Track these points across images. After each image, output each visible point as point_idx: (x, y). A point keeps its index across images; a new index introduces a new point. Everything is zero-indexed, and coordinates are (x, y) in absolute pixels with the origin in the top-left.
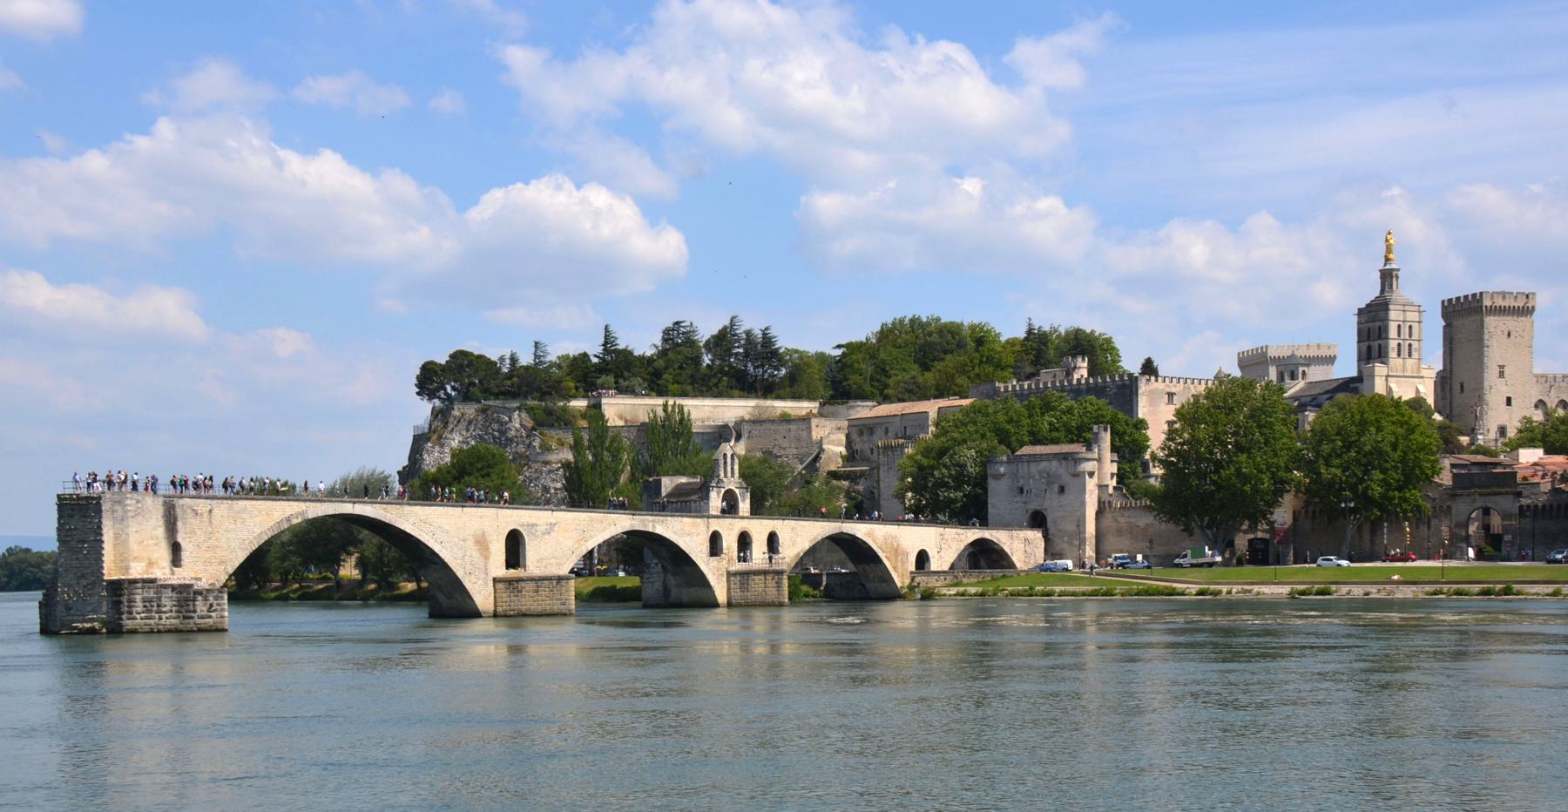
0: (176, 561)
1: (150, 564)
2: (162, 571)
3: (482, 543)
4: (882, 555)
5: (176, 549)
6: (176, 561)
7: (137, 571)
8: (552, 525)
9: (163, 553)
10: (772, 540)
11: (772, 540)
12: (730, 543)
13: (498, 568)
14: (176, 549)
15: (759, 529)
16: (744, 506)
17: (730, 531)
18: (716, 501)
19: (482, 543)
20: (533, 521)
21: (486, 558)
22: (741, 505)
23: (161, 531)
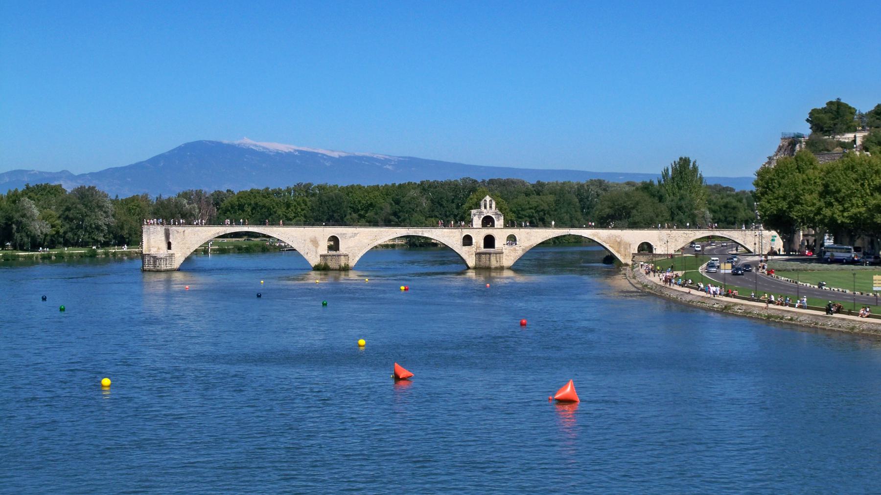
0: (169, 247)
1: (159, 249)
2: (163, 252)
3: (315, 242)
4: (607, 246)
6: (169, 247)
7: (153, 252)
8: (356, 234)
9: (165, 246)
10: (512, 239)
11: (512, 239)
13: (323, 249)
15: (500, 234)
16: (499, 222)
17: (478, 235)
18: (477, 221)
21: (317, 247)
22: (496, 222)
23: (163, 238)
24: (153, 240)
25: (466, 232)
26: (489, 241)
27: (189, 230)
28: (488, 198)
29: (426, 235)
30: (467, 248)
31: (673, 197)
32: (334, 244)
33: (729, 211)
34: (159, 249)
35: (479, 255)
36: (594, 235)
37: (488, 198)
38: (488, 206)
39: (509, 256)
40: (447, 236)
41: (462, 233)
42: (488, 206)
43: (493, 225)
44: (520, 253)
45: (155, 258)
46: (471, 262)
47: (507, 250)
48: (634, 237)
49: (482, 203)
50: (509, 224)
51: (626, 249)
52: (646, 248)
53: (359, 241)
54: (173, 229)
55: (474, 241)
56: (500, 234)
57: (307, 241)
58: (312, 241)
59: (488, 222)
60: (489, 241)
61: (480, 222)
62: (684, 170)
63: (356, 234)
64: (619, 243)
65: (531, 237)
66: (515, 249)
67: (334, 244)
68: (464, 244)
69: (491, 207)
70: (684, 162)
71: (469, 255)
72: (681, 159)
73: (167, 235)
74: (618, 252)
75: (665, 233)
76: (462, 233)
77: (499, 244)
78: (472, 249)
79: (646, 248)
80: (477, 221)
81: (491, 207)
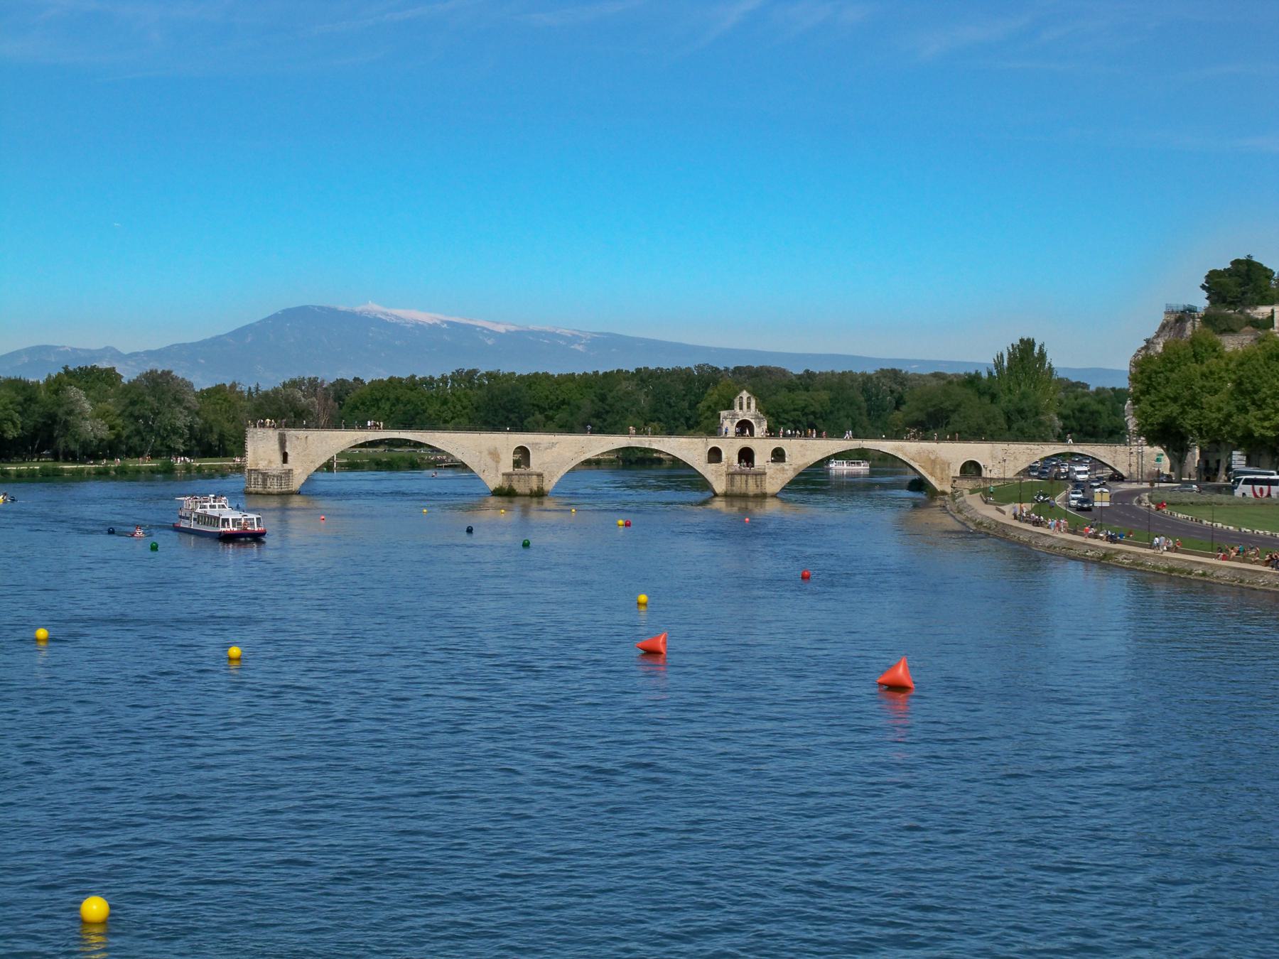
0: (285, 460)
1: (270, 462)
2: (276, 466)
3: (495, 455)
6: (285, 460)
7: (262, 465)
8: (553, 445)
9: (279, 458)
10: (778, 455)
11: (778, 455)
13: (507, 465)
16: (760, 430)
17: (730, 448)
18: (729, 425)
21: (498, 462)
22: (756, 430)
23: (277, 447)
24: (261, 448)
25: (713, 442)
26: (746, 455)
27: (314, 435)
28: (745, 394)
29: (655, 447)
31: (1014, 395)
32: (523, 455)
33: (1090, 417)
34: (270, 462)
35: (731, 475)
36: (897, 449)
37: (745, 394)
38: (745, 406)
39: (776, 478)
40: (687, 449)
41: (707, 445)
42: (745, 406)
43: (752, 434)
44: (790, 475)
45: (265, 476)
46: (720, 486)
47: (771, 469)
48: (956, 453)
49: (737, 401)
50: (772, 432)
51: (943, 470)
52: (971, 469)
53: (559, 453)
54: (291, 433)
55: (724, 456)
56: (762, 447)
57: (484, 452)
59: (744, 427)
60: (746, 455)
62: (1026, 357)
63: (553, 445)
64: (934, 462)
65: (805, 451)
66: (783, 469)
67: (523, 455)
68: (710, 461)
69: (749, 407)
70: (1027, 345)
71: (717, 477)
72: (1022, 341)
73: (282, 442)
74: (932, 475)
75: (1000, 447)
76: (707, 445)
77: (762, 459)
78: (722, 467)
79: (971, 469)
80: (729, 426)
81: (749, 407)
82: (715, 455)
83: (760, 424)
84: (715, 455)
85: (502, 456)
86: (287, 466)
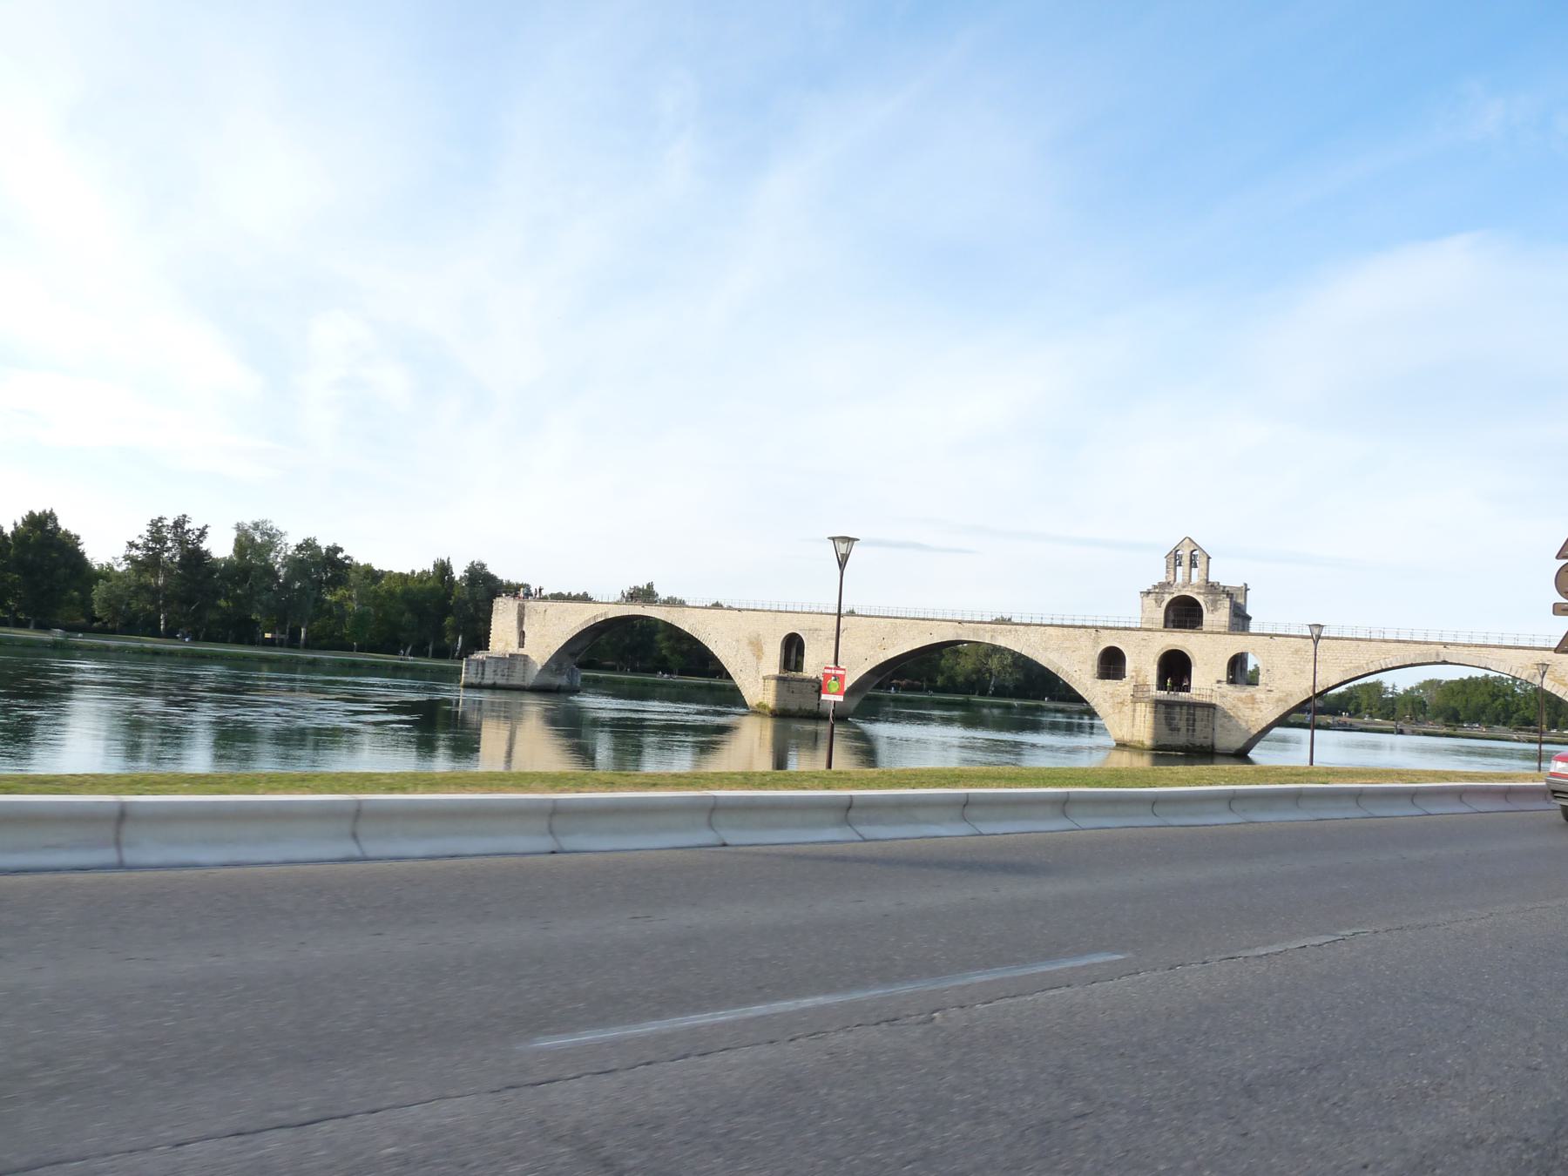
0: (521, 645)
2: (514, 648)
3: (756, 646)
5: (522, 634)
6: (521, 645)
12: (1143, 664)
13: (772, 662)
14: (522, 634)
19: (756, 646)
20: (816, 625)
21: (759, 658)
22: (1207, 616)
23: (515, 623)
26: (1175, 668)
30: (1110, 685)
41: (1096, 641)
55: (1129, 666)
58: (751, 643)
60: (1175, 668)
61: (1160, 615)
66: (1253, 700)
77: (1206, 681)
78: (1123, 687)
82: (1111, 664)
83: (1215, 609)
84: (1111, 664)
85: (765, 648)
86: (522, 651)
